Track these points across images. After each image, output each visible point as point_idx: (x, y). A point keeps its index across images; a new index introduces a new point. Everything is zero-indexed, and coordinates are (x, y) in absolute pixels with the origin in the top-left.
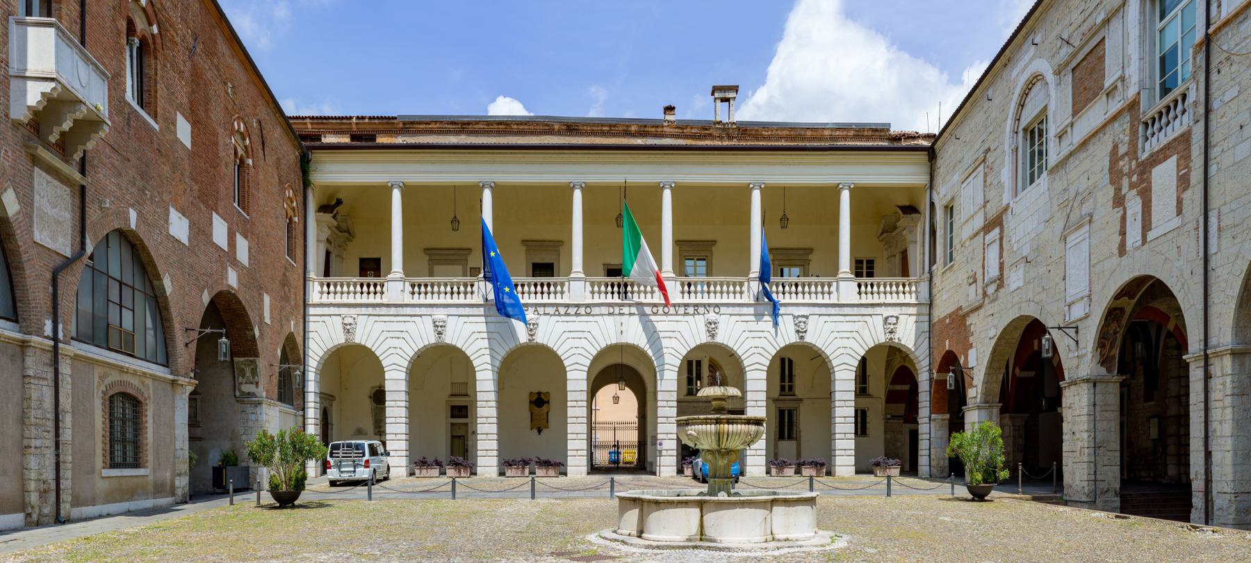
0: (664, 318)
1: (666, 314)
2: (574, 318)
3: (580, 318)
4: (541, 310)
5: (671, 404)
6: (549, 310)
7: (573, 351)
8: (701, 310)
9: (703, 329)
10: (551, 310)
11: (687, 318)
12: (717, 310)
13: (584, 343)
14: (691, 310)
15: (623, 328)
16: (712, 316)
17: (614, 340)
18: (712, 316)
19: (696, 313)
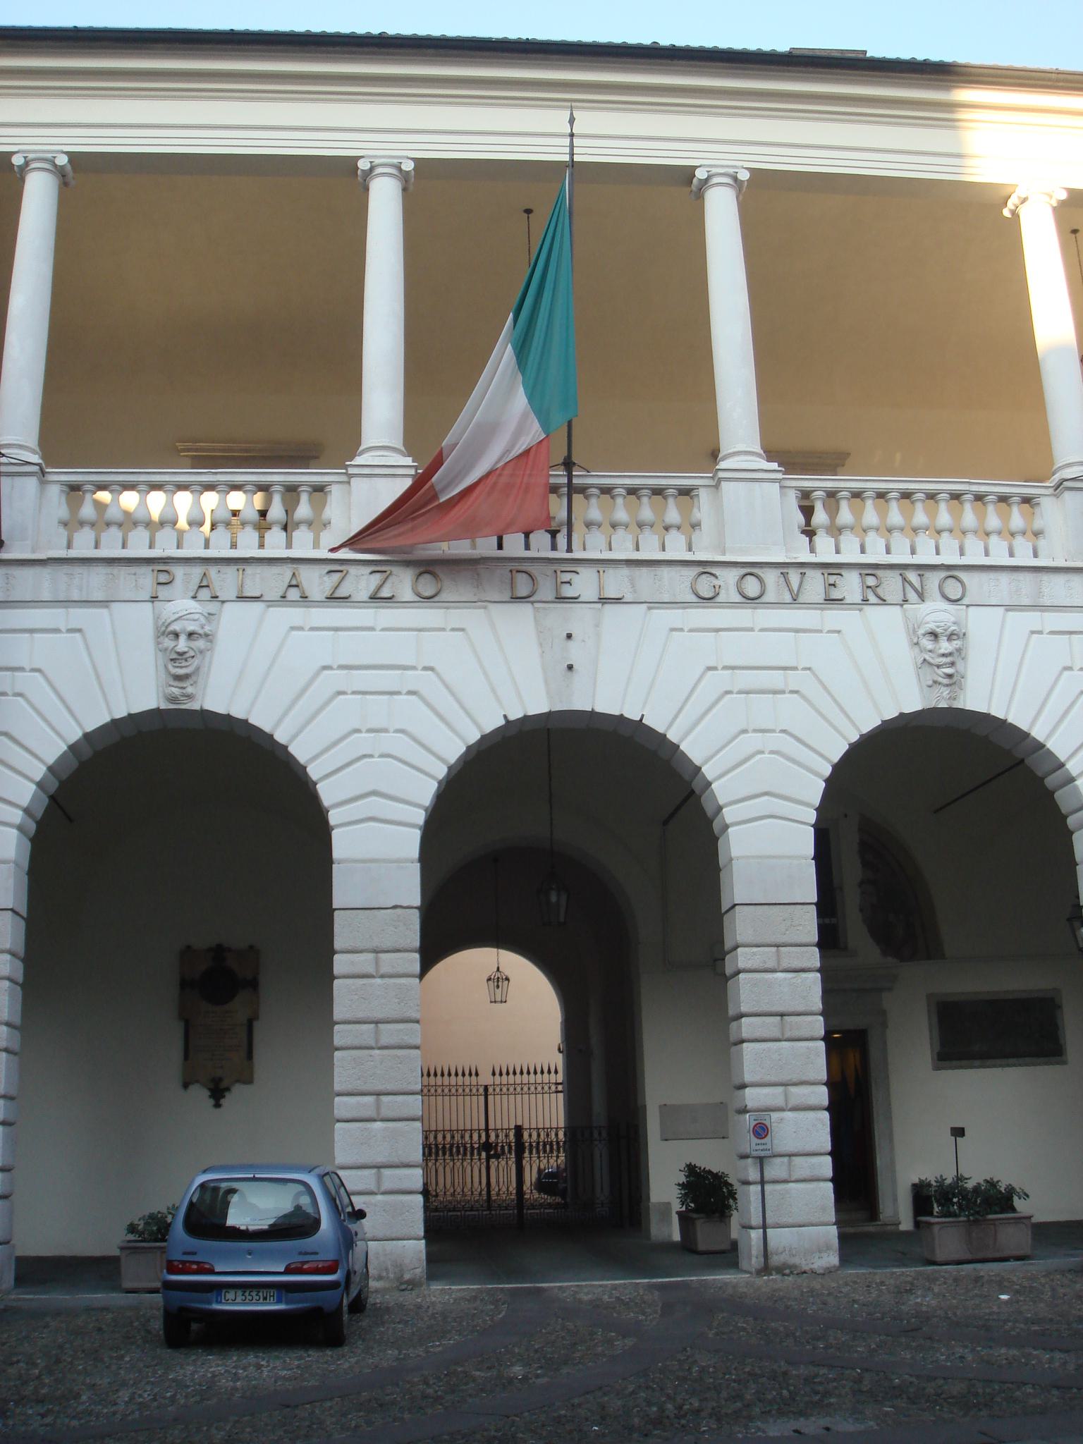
0: (744, 616)
1: (752, 601)
2: (366, 615)
3: (387, 616)
4: (225, 580)
5: (794, 957)
6: (257, 581)
7: (363, 742)
8: (891, 584)
9: (902, 657)
10: (271, 581)
11: (834, 617)
12: (953, 589)
13: (408, 712)
14: (851, 585)
15: (576, 653)
16: (935, 612)
17: (535, 700)
18: (935, 612)
19: (873, 597)
